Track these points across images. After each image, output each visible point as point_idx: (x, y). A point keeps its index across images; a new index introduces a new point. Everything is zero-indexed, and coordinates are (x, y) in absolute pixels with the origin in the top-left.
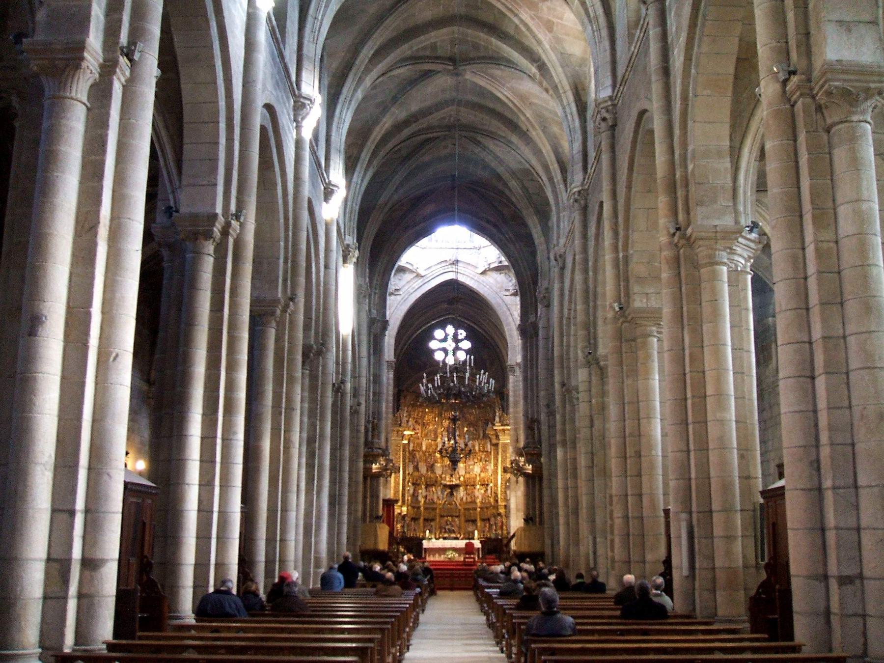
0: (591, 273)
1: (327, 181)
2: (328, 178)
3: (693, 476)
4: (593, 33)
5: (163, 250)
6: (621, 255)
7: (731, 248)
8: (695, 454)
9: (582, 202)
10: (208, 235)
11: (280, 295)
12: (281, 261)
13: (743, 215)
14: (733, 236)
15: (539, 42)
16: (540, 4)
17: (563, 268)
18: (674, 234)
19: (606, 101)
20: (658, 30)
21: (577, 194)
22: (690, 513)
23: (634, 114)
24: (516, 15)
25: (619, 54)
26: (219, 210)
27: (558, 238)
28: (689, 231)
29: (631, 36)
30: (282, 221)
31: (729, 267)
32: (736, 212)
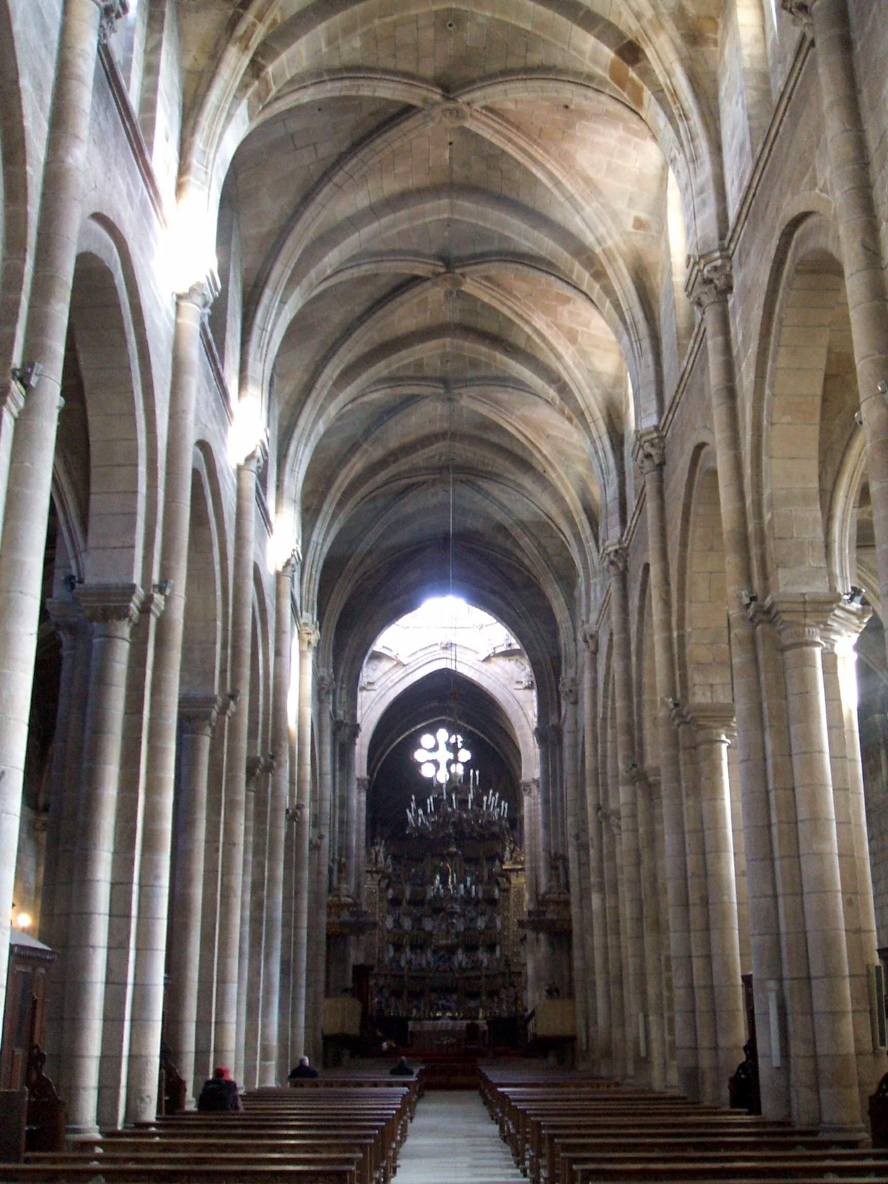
0: (634, 659)
4: (632, 345)
5: (61, 633)
6: (675, 634)
7: (826, 624)
9: (620, 565)
10: (122, 613)
11: (216, 692)
12: (218, 647)
13: (839, 580)
14: (827, 607)
15: (559, 357)
16: (560, 308)
17: (595, 652)
18: (748, 605)
20: (720, 339)
23: (689, 448)
24: (528, 323)
26: (137, 579)
27: (588, 612)
29: (681, 347)
30: (219, 593)
32: (831, 576)
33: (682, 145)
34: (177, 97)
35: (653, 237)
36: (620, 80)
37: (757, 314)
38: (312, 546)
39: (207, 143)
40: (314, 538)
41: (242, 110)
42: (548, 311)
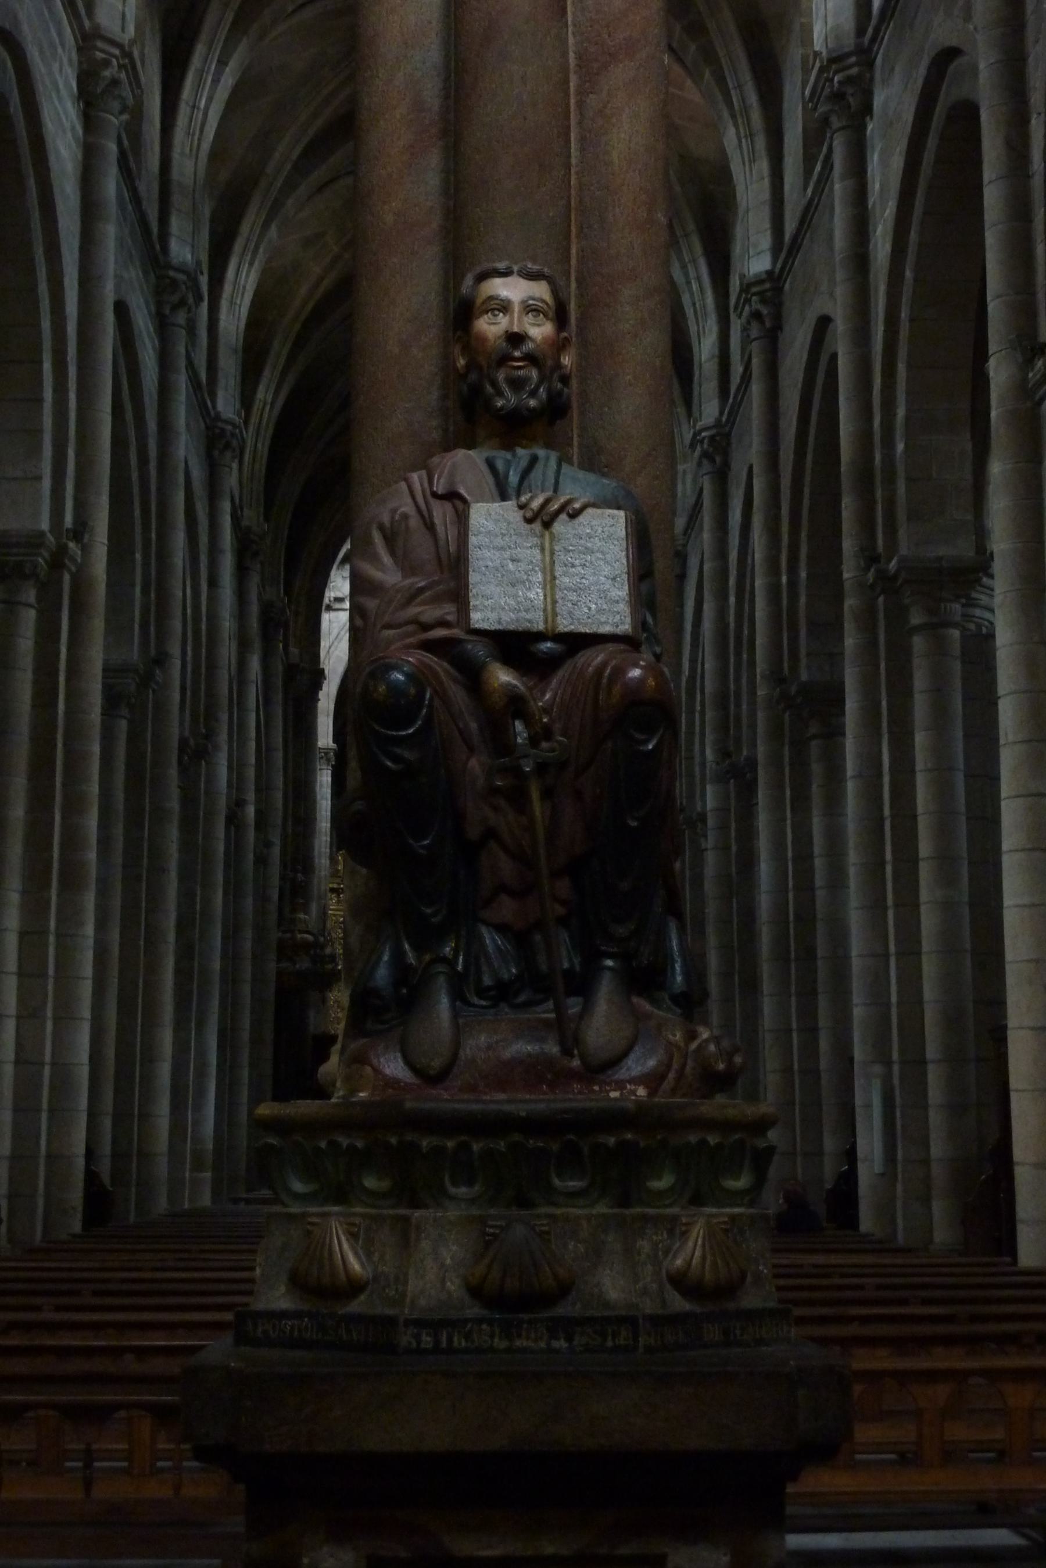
0: (732, 599)
1: (212, 413)
2: (214, 407)
3: (894, 999)
4: (740, 142)
6: (784, 579)
7: (968, 597)
8: (897, 960)
9: (718, 459)
12: (138, 590)
21: (706, 441)
25: (787, 187)
26: (45, 525)
28: (893, 564)
30: (137, 513)
31: (964, 629)
37: (897, 162)
38: (257, 406)
40: (260, 394)
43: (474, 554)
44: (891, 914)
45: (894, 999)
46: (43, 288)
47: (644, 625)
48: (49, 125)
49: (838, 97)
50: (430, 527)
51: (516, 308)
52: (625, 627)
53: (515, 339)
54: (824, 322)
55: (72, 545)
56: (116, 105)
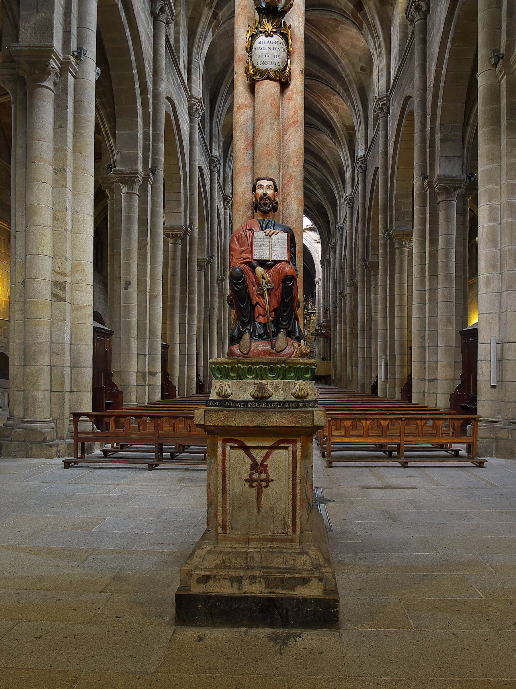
0: (354, 240)
2: (225, 192)
7: (410, 240)
15: (332, 118)
17: (342, 234)
19: (362, 158)
22: (386, 355)
24: (319, 103)
26: (183, 224)
27: (340, 218)
33: (376, 49)
34: (186, 31)
35: (368, 74)
36: (356, 18)
37: (395, 127)
39: (198, 50)
41: (210, 33)
42: (328, 98)
43: (255, 243)
44: (388, 319)
45: (388, 340)
46: (180, 164)
47: (291, 258)
48: (181, 121)
49: (381, 109)
50: (247, 237)
51: (265, 187)
52: (286, 259)
53: (265, 194)
54: (377, 168)
55: (189, 229)
56: (198, 116)
